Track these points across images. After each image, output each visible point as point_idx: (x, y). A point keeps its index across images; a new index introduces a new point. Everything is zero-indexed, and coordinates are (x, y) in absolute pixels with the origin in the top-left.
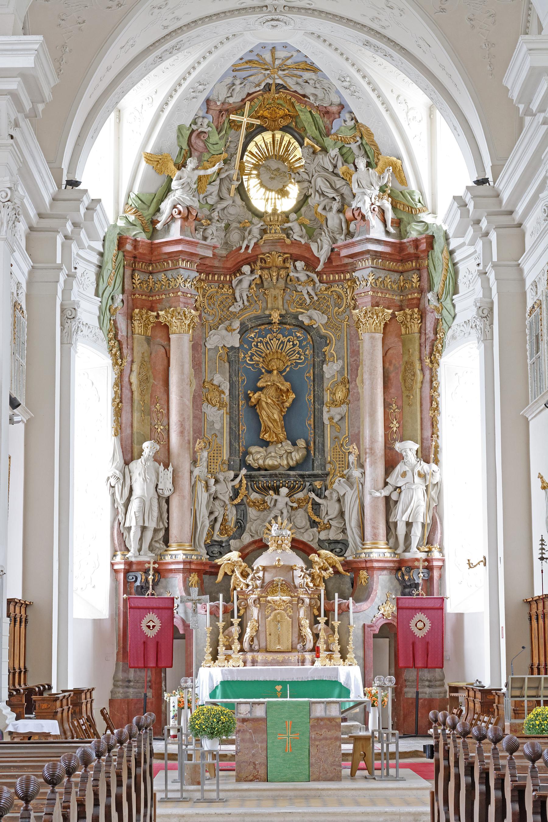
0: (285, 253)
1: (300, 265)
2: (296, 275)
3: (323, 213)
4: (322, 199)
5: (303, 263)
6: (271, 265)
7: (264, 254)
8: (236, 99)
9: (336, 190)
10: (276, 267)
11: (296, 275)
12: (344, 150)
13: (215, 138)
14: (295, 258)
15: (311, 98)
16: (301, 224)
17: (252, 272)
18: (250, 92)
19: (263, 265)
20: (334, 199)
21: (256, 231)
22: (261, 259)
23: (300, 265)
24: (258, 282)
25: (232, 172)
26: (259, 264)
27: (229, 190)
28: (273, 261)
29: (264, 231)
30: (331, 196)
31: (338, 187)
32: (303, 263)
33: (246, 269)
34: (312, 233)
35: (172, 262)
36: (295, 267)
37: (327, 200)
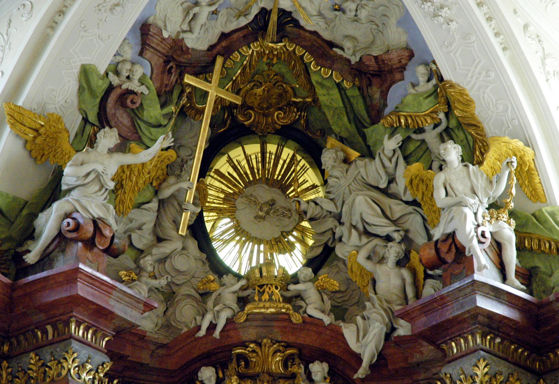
0: (288, 346)
3: (368, 266)
5: (325, 366)
6: (258, 369)
7: (244, 345)
8: (198, 41)
9: (395, 222)
10: (270, 374)
12: (412, 147)
13: (153, 111)
14: (307, 357)
15: (347, 44)
16: (321, 291)
18: (227, 31)
19: (242, 370)
21: (230, 299)
22: (240, 357)
25: (184, 185)
26: (234, 365)
27: (176, 224)
28: (265, 361)
29: (243, 301)
30: (382, 231)
31: (397, 215)
32: (325, 366)
34: (344, 307)
35: (55, 328)
37: (376, 241)
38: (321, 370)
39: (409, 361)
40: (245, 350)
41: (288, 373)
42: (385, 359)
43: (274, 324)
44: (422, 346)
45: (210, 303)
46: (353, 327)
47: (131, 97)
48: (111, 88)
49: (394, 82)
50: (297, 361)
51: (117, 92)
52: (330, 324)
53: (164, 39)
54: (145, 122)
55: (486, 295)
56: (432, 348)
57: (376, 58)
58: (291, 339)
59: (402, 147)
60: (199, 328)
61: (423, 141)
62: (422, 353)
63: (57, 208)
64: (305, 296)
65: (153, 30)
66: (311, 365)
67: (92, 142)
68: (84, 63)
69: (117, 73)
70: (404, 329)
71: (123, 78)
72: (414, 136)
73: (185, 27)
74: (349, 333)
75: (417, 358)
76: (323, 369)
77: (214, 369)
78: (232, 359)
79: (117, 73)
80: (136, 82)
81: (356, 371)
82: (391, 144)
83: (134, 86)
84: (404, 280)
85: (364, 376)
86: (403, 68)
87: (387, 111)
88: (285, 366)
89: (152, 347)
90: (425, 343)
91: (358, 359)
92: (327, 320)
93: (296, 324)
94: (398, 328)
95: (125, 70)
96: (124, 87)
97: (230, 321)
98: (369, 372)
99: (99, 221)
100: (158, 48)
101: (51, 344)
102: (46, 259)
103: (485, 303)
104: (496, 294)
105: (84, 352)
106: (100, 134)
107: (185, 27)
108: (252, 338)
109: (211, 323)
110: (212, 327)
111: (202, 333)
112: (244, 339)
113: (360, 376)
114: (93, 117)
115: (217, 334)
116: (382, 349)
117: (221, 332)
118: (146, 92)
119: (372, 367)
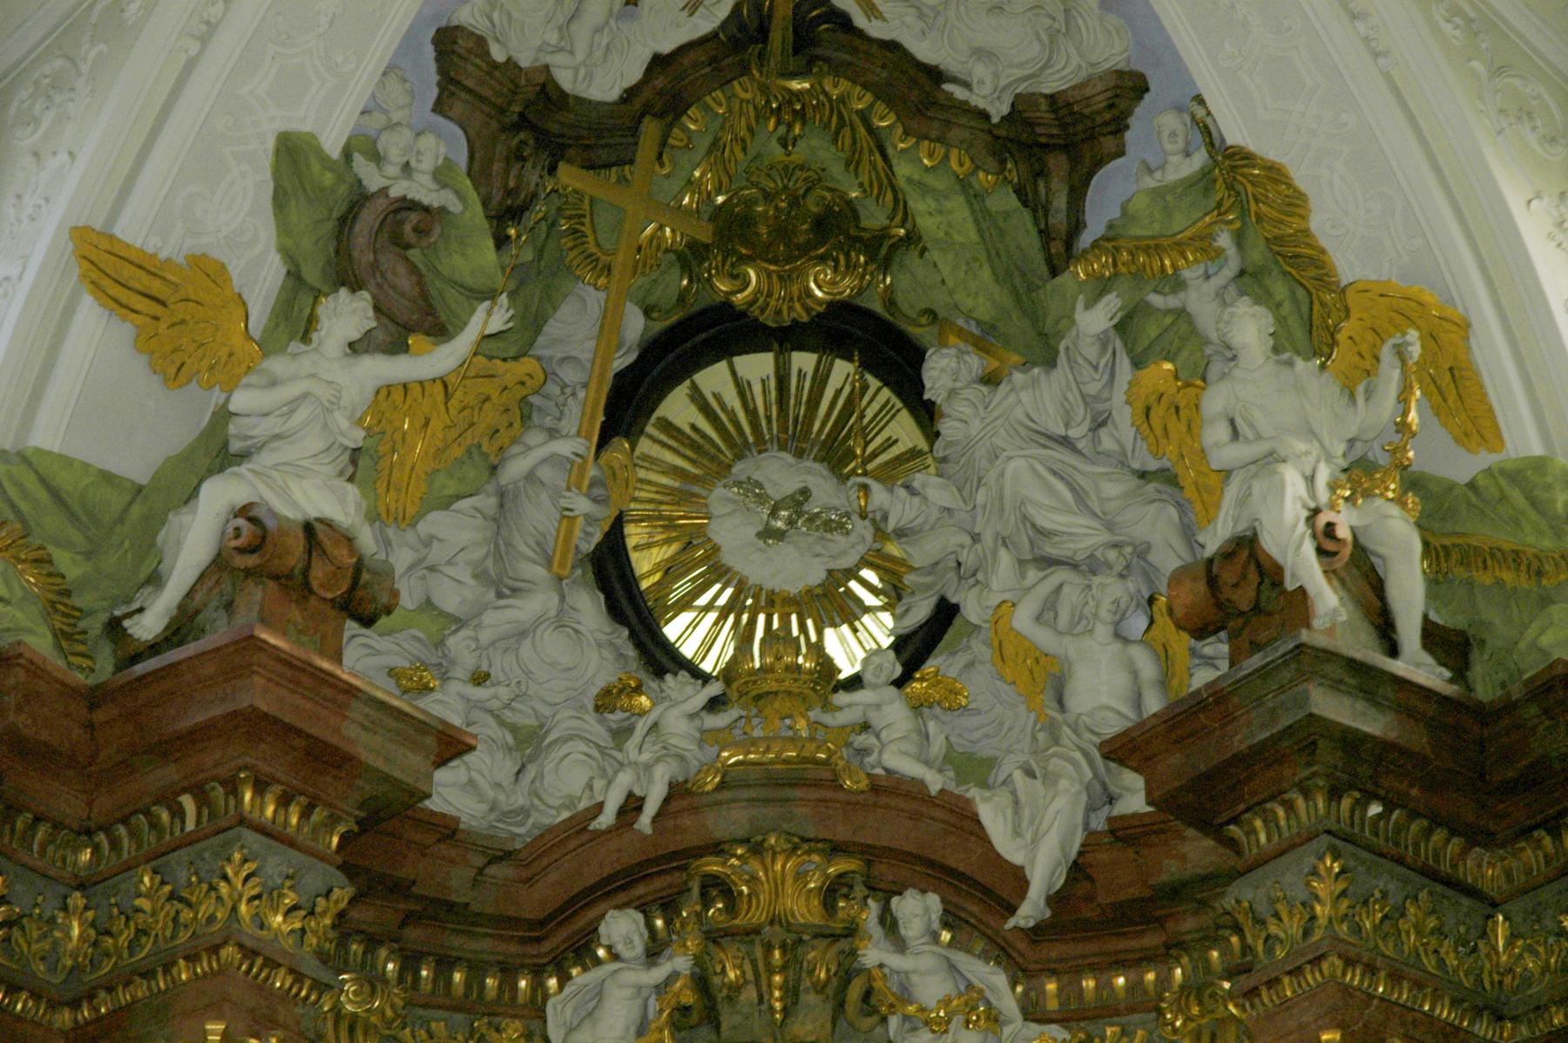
0: (836, 849)
1: (918, 909)
2: (895, 961)
3: (1043, 638)
4: (1032, 574)
5: (934, 901)
7: (718, 849)
11: (895, 961)
17: (655, 951)
20: (1090, 567)
23: (918, 909)
24: (689, 998)
30: (1079, 548)
32: (934, 901)
33: (621, 928)
35: (203, 800)
36: (889, 923)
38: (920, 912)
39: (1152, 882)
40: (724, 864)
41: (838, 926)
42: (1092, 880)
43: (798, 793)
44: (1184, 839)
45: (631, 744)
46: (1003, 798)
47: (414, 217)
48: (360, 199)
49: (1098, 164)
50: (860, 890)
51: (380, 204)
52: (942, 791)
53: (495, 66)
54: (454, 283)
55: (1336, 686)
56: (1209, 843)
57: (1052, 98)
58: (842, 833)
59: (1123, 327)
60: (599, 807)
61: (1181, 313)
62: (1183, 858)
63: (219, 496)
64: (875, 719)
65: (463, 44)
66: (895, 900)
67: (306, 330)
68: (283, 129)
69: (376, 157)
70: (1134, 798)
71: (392, 170)
72: (1156, 300)
73: (553, 37)
74: (993, 817)
75: (1171, 871)
76: (927, 910)
77: (640, 917)
78: (689, 890)
79: (376, 157)
80: (426, 180)
81: (1012, 910)
82: (1095, 320)
83: (422, 190)
84: (1135, 674)
85: (1031, 923)
86: (1119, 126)
87: (1085, 239)
88: (829, 905)
89: (479, 861)
90: (1191, 832)
91: (1019, 879)
92: (935, 782)
93: (850, 791)
94: (1120, 796)
95: (394, 146)
96: (395, 192)
97: (677, 792)
98: (1048, 914)
99: (318, 526)
100: (485, 91)
101: (190, 841)
102: (181, 628)
103: (1334, 707)
104: (1366, 681)
105: (277, 863)
106: (325, 307)
107: (553, 37)
108: (741, 833)
109: (630, 795)
110: (632, 806)
111: (606, 819)
112: (719, 834)
113: (1022, 923)
114: (312, 275)
115: (645, 822)
116: (1080, 854)
117: (656, 819)
118: (455, 206)
119: (1056, 900)
